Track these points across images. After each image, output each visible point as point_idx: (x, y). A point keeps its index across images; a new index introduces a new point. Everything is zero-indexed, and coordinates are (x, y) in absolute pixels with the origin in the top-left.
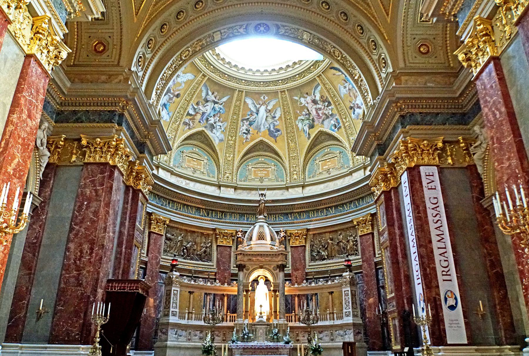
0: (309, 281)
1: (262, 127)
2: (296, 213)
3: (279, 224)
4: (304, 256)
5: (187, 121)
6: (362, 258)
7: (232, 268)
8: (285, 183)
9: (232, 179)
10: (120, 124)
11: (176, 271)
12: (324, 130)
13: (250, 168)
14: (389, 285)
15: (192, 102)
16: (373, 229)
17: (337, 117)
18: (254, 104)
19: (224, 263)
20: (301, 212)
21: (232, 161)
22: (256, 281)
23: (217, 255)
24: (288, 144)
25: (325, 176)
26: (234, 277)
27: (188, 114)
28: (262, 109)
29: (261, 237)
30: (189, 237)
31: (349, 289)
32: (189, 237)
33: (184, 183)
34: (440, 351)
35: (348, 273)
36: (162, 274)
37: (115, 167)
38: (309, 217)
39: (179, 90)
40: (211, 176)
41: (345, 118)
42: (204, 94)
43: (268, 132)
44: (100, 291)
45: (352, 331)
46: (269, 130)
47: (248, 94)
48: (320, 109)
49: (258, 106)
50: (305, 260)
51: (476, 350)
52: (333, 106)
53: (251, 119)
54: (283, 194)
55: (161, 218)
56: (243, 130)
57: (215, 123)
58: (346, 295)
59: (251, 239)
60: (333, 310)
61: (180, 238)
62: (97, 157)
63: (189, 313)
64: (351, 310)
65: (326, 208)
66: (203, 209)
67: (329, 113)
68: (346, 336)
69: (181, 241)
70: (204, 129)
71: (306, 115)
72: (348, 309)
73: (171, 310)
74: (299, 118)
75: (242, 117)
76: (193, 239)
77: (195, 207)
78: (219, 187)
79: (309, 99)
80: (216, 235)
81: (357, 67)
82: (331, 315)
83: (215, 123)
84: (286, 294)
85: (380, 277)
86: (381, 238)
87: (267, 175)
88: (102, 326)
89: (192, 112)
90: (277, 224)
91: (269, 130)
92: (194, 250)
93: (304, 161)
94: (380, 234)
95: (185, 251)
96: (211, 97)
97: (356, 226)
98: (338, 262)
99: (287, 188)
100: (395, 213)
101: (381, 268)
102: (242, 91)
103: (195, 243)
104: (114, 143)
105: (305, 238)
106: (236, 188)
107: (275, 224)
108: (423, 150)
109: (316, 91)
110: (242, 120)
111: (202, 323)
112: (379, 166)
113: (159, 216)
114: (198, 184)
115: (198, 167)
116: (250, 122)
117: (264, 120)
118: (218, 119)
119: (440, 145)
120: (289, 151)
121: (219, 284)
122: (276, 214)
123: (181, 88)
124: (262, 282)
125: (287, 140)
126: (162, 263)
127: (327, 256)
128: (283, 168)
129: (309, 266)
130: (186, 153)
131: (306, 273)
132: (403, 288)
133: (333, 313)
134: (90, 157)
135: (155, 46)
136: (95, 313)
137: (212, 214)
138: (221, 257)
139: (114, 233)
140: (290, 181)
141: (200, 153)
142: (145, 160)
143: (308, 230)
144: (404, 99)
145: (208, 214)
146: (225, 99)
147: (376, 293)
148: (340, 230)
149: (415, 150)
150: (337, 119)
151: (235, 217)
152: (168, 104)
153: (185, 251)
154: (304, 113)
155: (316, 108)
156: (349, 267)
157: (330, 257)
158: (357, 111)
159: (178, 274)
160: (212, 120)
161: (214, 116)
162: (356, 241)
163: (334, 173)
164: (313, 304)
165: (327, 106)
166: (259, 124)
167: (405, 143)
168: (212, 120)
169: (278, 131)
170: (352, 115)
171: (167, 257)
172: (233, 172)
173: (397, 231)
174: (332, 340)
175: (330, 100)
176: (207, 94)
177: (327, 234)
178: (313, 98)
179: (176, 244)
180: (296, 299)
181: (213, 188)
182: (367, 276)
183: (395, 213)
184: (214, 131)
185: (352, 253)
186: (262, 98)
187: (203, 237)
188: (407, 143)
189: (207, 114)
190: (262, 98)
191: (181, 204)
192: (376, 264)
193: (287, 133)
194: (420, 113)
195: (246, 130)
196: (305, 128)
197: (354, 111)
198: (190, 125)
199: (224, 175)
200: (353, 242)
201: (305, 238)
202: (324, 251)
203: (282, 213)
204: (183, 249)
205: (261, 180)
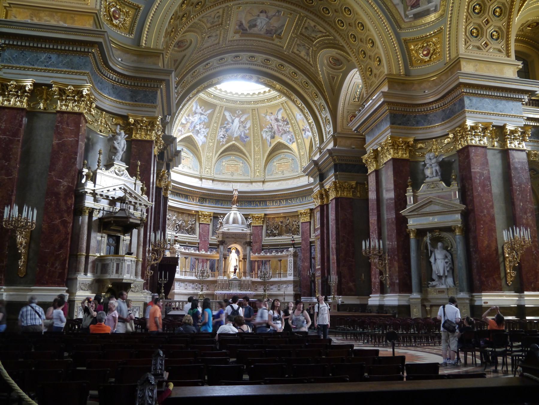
0: (264, 250)
1: (235, 134)
2: (257, 201)
3: (244, 209)
4: (262, 233)
6: (302, 237)
7: (210, 240)
8: (250, 178)
9: (211, 173)
12: (282, 141)
13: (224, 164)
14: (318, 256)
15: (185, 115)
16: (310, 219)
17: (293, 134)
18: (230, 116)
19: (204, 236)
20: (261, 201)
21: (211, 159)
22: (229, 250)
23: (200, 229)
24: (254, 148)
25: (280, 176)
26: (213, 247)
27: (182, 124)
28: (237, 121)
29: (235, 221)
31: (292, 259)
34: (340, 298)
35: (292, 249)
38: (266, 205)
40: (195, 169)
41: (299, 136)
42: (194, 109)
43: (239, 138)
45: (292, 285)
46: (240, 136)
47: (227, 109)
48: (281, 126)
49: (234, 118)
50: (262, 236)
51: (358, 298)
52: (290, 126)
53: (227, 127)
54: (248, 186)
56: (221, 135)
57: (200, 129)
58: (290, 263)
59: (227, 222)
60: (281, 271)
61: (174, 218)
63: (185, 272)
64: (292, 272)
65: (279, 200)
66: (190, 196)
67: (286, 130)
68: (288, 288)
71: (270, 128)
72: (291, 270)
73: (177, 270)
74: (264, 130)
75: (221, 125)
76: (183, 218)
77: (184, 195)
78: (201, 179)
79: (273, 117)
80: (199, 215)
81: (311, 116)
82: (279, 275)
83: (200, 129)
84: (251, 259)
85: (312, 251)
86: (316, 232)
87: (237, 170)
88: (165, 284)
89: (184, 121)
90: (243, 209)
91: (240, 136)
92: (184, 226)
93: (266, 161)
94: (315, 230)
95: (178, 227)
96: (199, 110)
97: (299, 215)
98: (285, 239)
99: (251, 182)
100: (325, 219)
101: (314, 245)
102: (223, 107)
103: (184, 221)
104: (162, 174)
105: (263, 220)
106: (213, 180)
107: (241, 209)
108: (345, 188)
109: (279, 113)
110: (220, 128)
111: (194, 278)
112: (319, 189)
116: (226, 129)
117: (238, 127)
119: (354, 186)
120: (254, 154)
121: (204, 252)
122: (242, 201)
124: (234, 251)
125: (254, 145)
127: (278, 234)
128: (248, 166)
129: (265, 240)
131: (263, 245)
132: (326, 264)
133: (280, 273)
137: (196, 200)
138: (202, 231)
140: (254, 177)
143: (265, 215)
144: (337, 156)
145: (193, 200)
146: (209, 112)
147: (309, 261)
148: (288, 216)
149: (340, 188)
150: (292, 135)
151: (212, 202)
153: (178, 227)
154: (268, 126)
155: (277, 125)
156: (293, 245)
157: (280, 234)
158: (307, 133)
160: (198, 127)
161: (200, 124)
162: (299, 225)
163: (287, 174)
164: (268, 266)
165: (286, 125)
166: (233, 131)
167: (335, 183)
168: (198, 127)
169: (247, 138)
170: (304, 135)
172: (211, 168)
173: (325, 231)
174: (279, 290)
175: (289, 121)
176: (197, 108)
177: (279, 219)
178: (276, 117)
179: (172, 221)
180: (256, 263)
181: (197, 180)
182: (304, 250)
183: (325, 219)
184: (199, 135)
185: (295, 233)
186: (237, 112)
187: (190, 217)
188: (336, 182)
189: (195, 123)
190: (237, 112)
192: (311, 242)
193: (254, 140)
194: (346, 164)
195: (223, 135)
196: (268, 138)
197: (305, 133)
198: (182, 131)
199: (205, 169)
200: (296, 226)
201: (263, 221)
202: (275, 230)
203: (247, 201)
204: (177, 226)
205: (232, 174)
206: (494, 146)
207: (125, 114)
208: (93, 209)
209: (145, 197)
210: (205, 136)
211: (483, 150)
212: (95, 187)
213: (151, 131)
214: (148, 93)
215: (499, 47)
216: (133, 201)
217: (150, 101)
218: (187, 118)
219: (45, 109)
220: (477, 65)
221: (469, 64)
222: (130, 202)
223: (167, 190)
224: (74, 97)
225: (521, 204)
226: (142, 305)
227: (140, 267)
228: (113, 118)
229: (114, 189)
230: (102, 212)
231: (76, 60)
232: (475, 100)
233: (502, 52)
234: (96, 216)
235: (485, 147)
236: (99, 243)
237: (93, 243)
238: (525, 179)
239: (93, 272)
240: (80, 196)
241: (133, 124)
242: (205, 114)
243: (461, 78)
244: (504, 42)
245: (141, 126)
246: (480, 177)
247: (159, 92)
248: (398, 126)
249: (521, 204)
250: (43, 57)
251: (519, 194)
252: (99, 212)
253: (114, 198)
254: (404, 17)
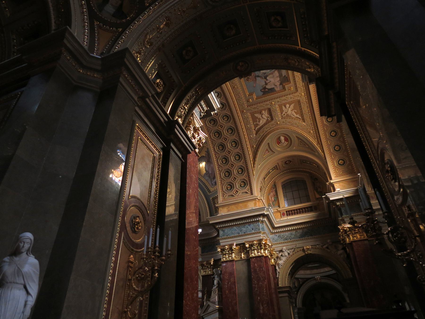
206: (241, 258)
211: (231, 263)
215: (246, 191)
220: (229, 207)
221: (224, 208)
225: (259, 298)
232: (226, 230)
233: (248, 193)
235: (232, 261)
238: (262, 277)
243: (210, 221)
244: (248, 187)
246: (228, 283)
248: (206, 253)
249: (259, 298)
251: (257, 291)
254: (211, 186)
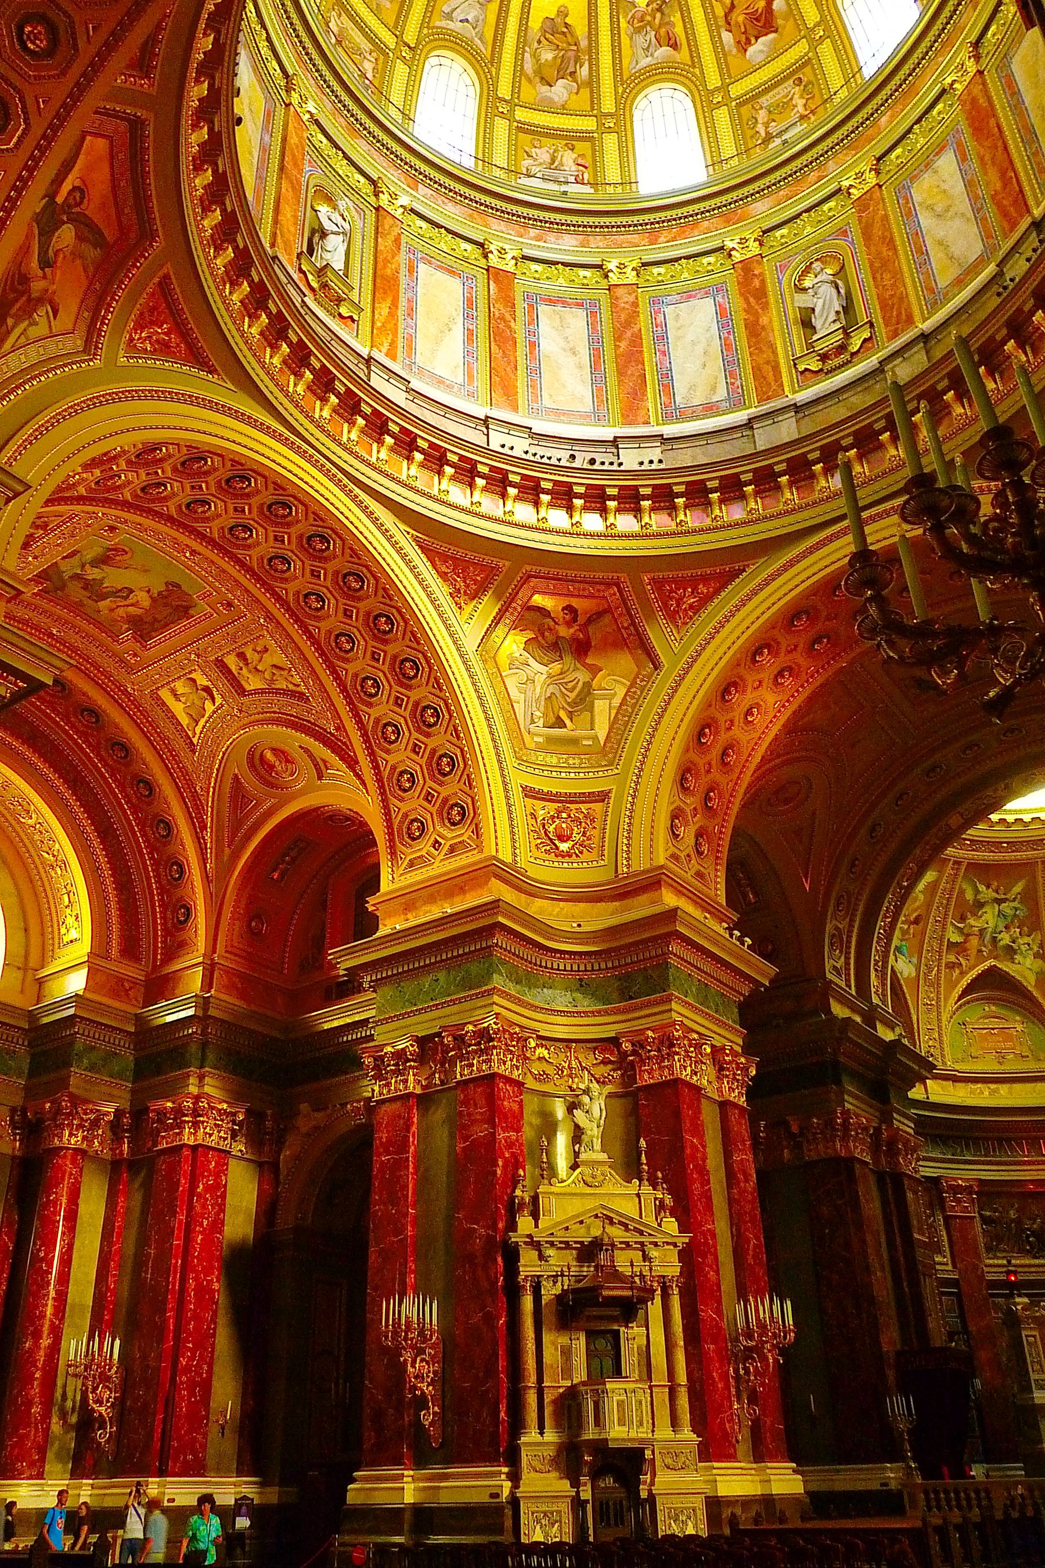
5: (952, 958)
10: (838, 1082)
11: (1019, 1296)
27: (951, 945)
30: (1034, 1208)
32: (1034, 1208)
33: (986, 1093)
36: (997, 1300)
37: (853, 1159)
39: (916, 910)
44: (891, 1375)
55: (960, 1182)
61: (1013, 1214)
62: (821, 1147)
69: (1019, 1222)
70: (992, 962)
73: (1033, 1376)
89: (955, 938)
96: (986, 894)
113: (955, 1179)
114: (1017, 1087)
115: (1009, 1044)
118: (1018, 930)
123: (917, 904)
126: (989, 1277)
130: (972, 1024)
134: (810, 1150)
135: (849, 902)
136: (893, 1409)
139: (883, 1269)
141: (1003, 1012)
142: (895, 1115)
146: (1018, 888)
152: (904, 943)
159: (1026, 1300)
160: (1005, 939)
168: (1005, 939)
171: (996, 1262)
176: (977, 892)
191: (992, 1139)
198: (961, 964)
207: (612, 1034)
208: (539, 1277)
209: (671, 1225)
210: (1036, 956)
212: (537, 1226)
213: (671, 1055)
214: (650, 971)
216: (632, 1238)
217: (658, 988)
218: (961, 925)
219: (442, 1083)
222: (627, 1244)
223: (898, 1153)
224: (479, 1044)
226: (699, 1503)
227: (683, 1401)
228: (595, 1048)
229: (581, 1222)
230: (560, 1278)
231: (474, 968)
234: (550, 1291)
236: (567, 1353)
237: (551, 1355)
239: (558, 1425)
240: (512, 1256)
241: (634, 1053)
242: (1011, 895)
245: (650, 1051)
247: (673, 961)
250: (427, 981)
252: (555, 1283)
253: (581, 1243)
